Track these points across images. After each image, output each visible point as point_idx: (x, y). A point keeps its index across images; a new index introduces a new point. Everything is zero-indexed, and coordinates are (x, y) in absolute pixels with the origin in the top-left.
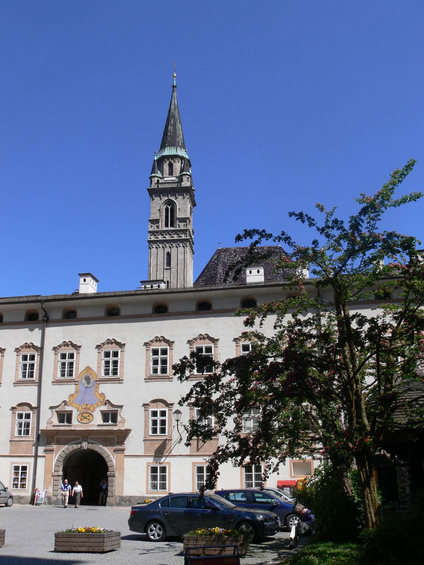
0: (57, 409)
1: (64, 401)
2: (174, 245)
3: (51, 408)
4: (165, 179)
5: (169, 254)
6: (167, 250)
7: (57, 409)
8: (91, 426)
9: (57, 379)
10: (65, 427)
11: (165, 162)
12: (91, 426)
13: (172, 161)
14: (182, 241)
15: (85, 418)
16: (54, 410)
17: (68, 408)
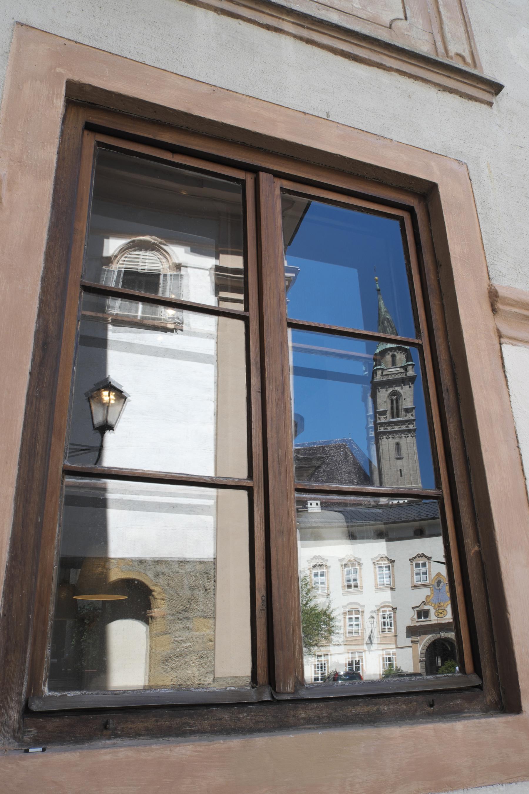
0: (418, 609)
1: (423, 602)
2: (403, 435)
3: (413, 608)
4: (390, 370)
5: (398, 444)
6: (397, 440)
7: (418, 609)
8: (445, 619)
9: (415, 584)
10: (423, 621)
11: (389, 354)
12: (445, 619)
13: (395, 353)
14: (409, 431)
15: (441, 613)
16: (415, 609)
17: (426, 607)
